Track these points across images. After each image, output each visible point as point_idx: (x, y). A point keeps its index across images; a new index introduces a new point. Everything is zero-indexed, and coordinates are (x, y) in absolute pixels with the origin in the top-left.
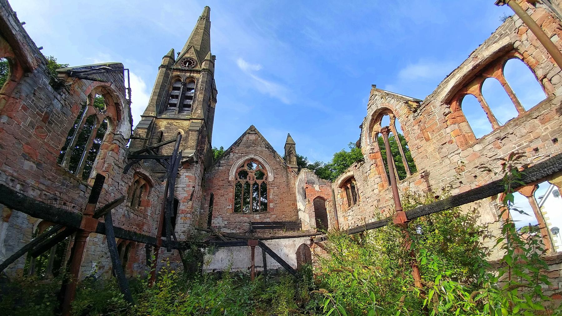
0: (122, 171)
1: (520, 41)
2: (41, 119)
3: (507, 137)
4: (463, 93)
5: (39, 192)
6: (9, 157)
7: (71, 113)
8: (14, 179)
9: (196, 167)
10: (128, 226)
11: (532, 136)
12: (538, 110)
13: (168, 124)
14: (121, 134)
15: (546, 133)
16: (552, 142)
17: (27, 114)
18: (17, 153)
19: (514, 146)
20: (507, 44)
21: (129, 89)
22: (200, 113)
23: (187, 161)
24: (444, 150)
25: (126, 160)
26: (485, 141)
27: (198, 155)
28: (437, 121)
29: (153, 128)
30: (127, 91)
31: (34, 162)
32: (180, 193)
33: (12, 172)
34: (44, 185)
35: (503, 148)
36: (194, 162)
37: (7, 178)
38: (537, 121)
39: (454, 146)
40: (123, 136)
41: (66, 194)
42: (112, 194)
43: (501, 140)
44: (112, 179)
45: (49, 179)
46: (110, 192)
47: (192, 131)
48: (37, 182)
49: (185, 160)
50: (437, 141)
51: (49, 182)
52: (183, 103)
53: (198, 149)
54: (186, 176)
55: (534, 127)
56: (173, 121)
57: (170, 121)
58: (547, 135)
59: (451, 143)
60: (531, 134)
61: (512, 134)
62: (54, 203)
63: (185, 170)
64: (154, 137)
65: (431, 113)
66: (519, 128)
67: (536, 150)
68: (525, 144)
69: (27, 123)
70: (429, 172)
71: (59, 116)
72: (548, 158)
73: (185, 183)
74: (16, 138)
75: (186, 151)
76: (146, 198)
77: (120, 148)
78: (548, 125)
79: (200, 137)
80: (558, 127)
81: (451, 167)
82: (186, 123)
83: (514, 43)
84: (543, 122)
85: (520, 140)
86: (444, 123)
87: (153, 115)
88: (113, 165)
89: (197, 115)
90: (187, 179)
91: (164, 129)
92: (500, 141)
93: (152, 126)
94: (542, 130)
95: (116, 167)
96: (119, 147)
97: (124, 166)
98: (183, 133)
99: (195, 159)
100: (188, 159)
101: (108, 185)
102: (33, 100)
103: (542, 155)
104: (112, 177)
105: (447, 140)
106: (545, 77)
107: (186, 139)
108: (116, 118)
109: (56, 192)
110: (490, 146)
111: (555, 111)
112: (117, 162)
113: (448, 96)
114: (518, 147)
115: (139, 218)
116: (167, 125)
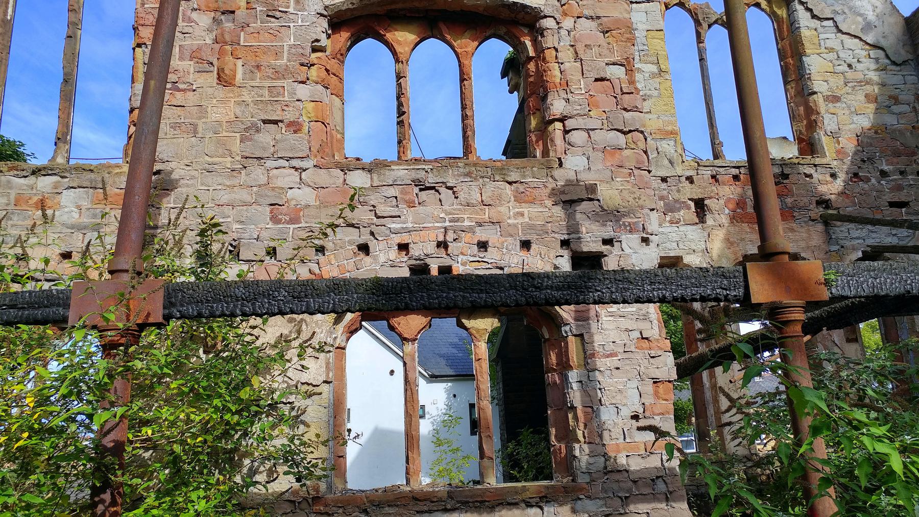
1: (558, 23)
3: (437, 191)
4: (377, 28)
11: (487, 214)
12: (522, 170)
15: (516, 222)
16: (518, 243)
19: (442, 215)
20: (534, 6)
24: (267, 137)
26: (387, 173)
28: (286, 48)
35: (420, 209)
38: (508, 190)
39: (297, 143)
43: (421, 190)
50: (256, 103)
55: (500, 198)
58: (515, 226)
59: (295, 132)
60: (487, 210)
61: (450, 188)
65: (278, 14)
66: (471, 183)
67: (483, 246)
68: (467, 223)
70: (177, 181)
72: (501, 272)
78: (526, 209)
80: (543, 223)
81: (261, 196)
83: (546, 17)
84: (520, 198)
85: (459, 210)
86: (302, 65)
92: (416, 190)
94: (511, 213)
103: (490, 261)
105: (289, 116)
106: (562, 120)
110: (392, 192)
111: (548, 191)
113: (350, 7)
114: (450, 222)
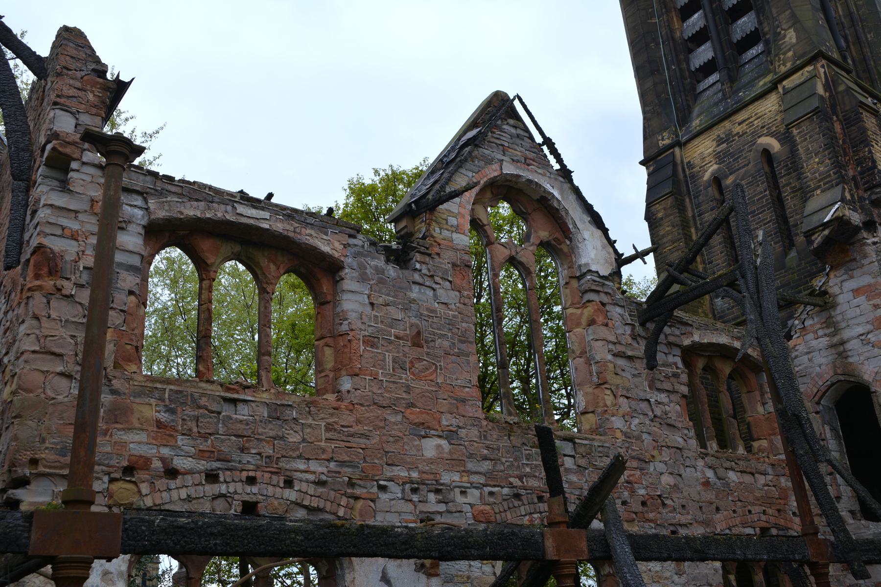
0: (641, 365)
2: (409, 343)
5: (476, 493)
6: (388, 448)
7: (458, 293)
8: (416, 485)
9: (874, 243)
10: (734, 512)
13: (720, 141)
14: (590, 271)
17: (380, 351)
18: (400, 434)
21: (548, 142)
22: (794, 41)
23: (827, 240)
25: (639, 329)
27: (861, 199)
29: (687, 181)
30: (545, 148)
31: (440, 437)
32: (862, 358)
33: (406, 474)
34: (480, 473)
36: (857, 229)
37: (403, 491)
40: (597, 272)
41: (535, 477)
42: (645, 436)
44: (628, 398)
45: (485, 458)
46: (635, 434)
47: (797, 122)
48: (463, 474)
49: (818, 239)
51: (487, 463)
52: (730, 41)
53: (851, 173)
54: (856, 292)
56: (727, 124)
57: (720, 131)
62: (516, 505)
63: (842, 271)
64: (703, 208)
69: (389, 366)
71: (439, 315)
73: (862, 319)
74: (384, 407)
75: (812, 205)
76: (760, 409)
77: (608, 308)
79: (838, 127)
82: (770, 105)
87: (667, 142)
88: (610, 362)
89: (790, 54)
90: (861, 299)
91: (715, 167)
93: (681, 176)
95: (621, 362)
96: (603, 304)
97: (640, 349)
98: (775, 145)
99: (856, 218)
100: (826, 232)
101: (623, 416)
102: (376, 317)
104: (624, 393)
107: (794, 164)
108: (559, 235)
109: (512, 480)
112: (619, 348)
115: (762, 480)
116: (719, 149)
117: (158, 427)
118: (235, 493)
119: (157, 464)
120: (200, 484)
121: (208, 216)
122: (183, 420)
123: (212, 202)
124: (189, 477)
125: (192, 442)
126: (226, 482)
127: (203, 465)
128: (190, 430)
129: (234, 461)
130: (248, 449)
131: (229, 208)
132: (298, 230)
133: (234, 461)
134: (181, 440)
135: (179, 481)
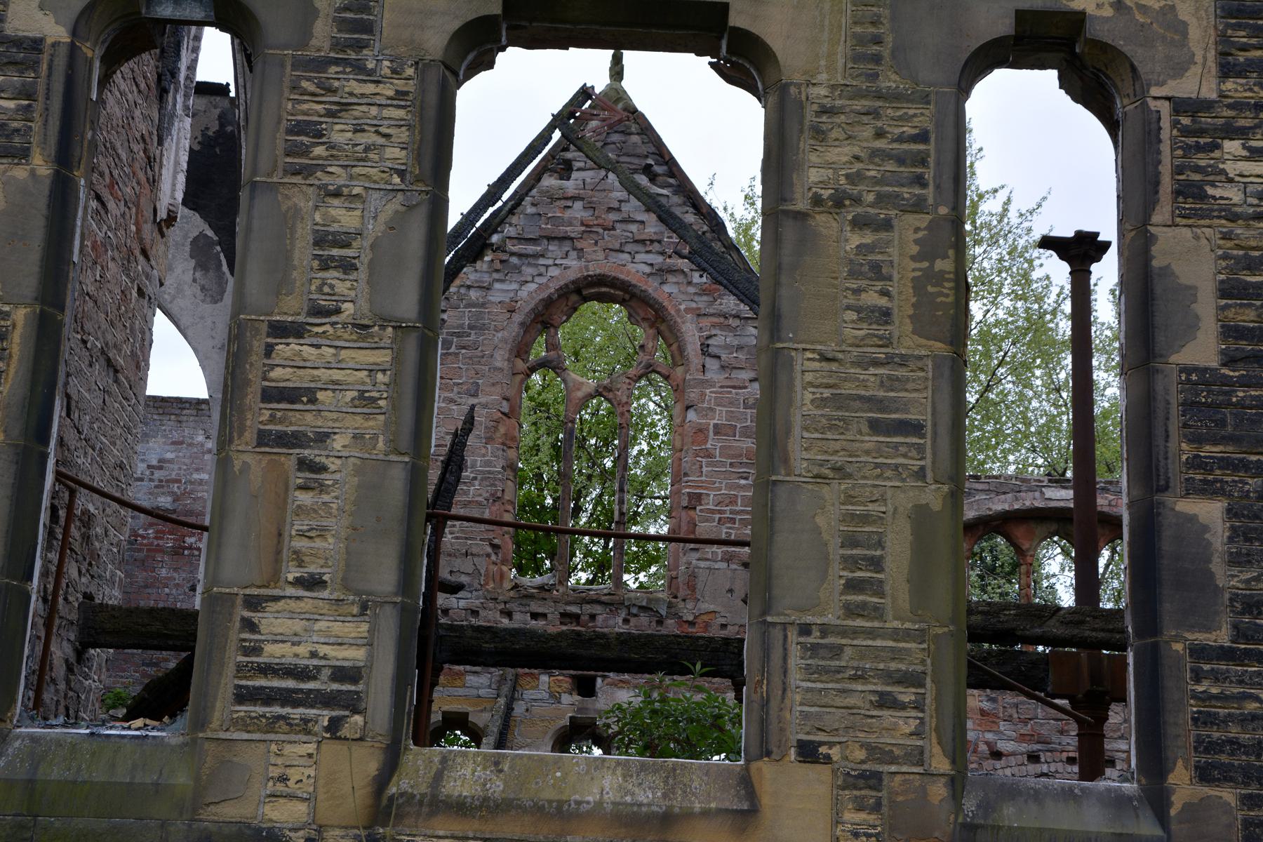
117: (982, 715)
118: (1057, 772)
119: (983, 748)
120: (1023, 764)
121: (1016, 507)
122: (1004, 707)
123: (1020, 492)
124: (1012, 758)
125: (1013, 727)
126: (1047, 762)
127: (1024, 747)
128: (1011, 716)
129: (1054, 743)
130: (1067, 731)
131: (1037, 494)
132: (1113, 503)
133: (1054, 743)
134: (1003, 726)
135: (1003, 762)
